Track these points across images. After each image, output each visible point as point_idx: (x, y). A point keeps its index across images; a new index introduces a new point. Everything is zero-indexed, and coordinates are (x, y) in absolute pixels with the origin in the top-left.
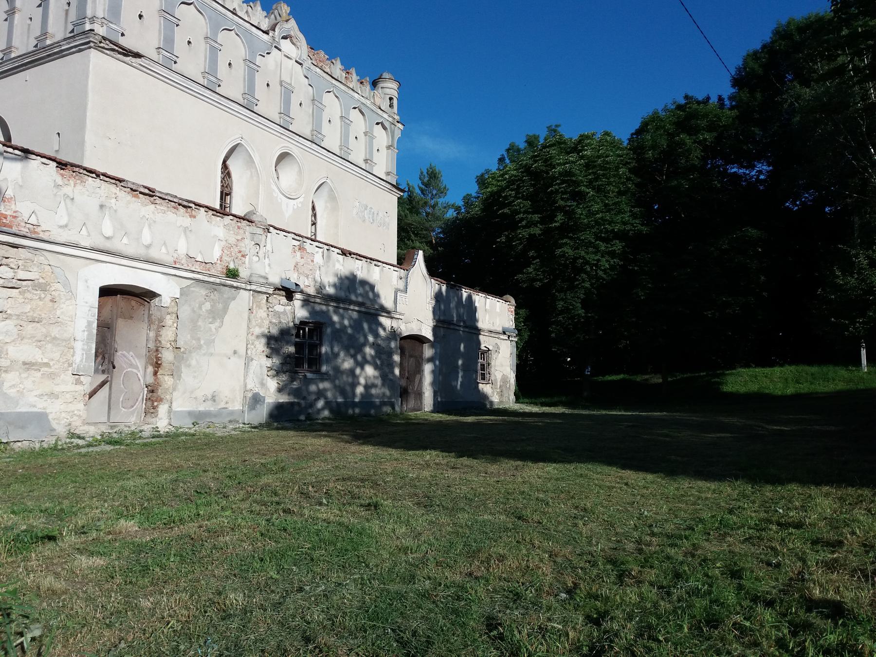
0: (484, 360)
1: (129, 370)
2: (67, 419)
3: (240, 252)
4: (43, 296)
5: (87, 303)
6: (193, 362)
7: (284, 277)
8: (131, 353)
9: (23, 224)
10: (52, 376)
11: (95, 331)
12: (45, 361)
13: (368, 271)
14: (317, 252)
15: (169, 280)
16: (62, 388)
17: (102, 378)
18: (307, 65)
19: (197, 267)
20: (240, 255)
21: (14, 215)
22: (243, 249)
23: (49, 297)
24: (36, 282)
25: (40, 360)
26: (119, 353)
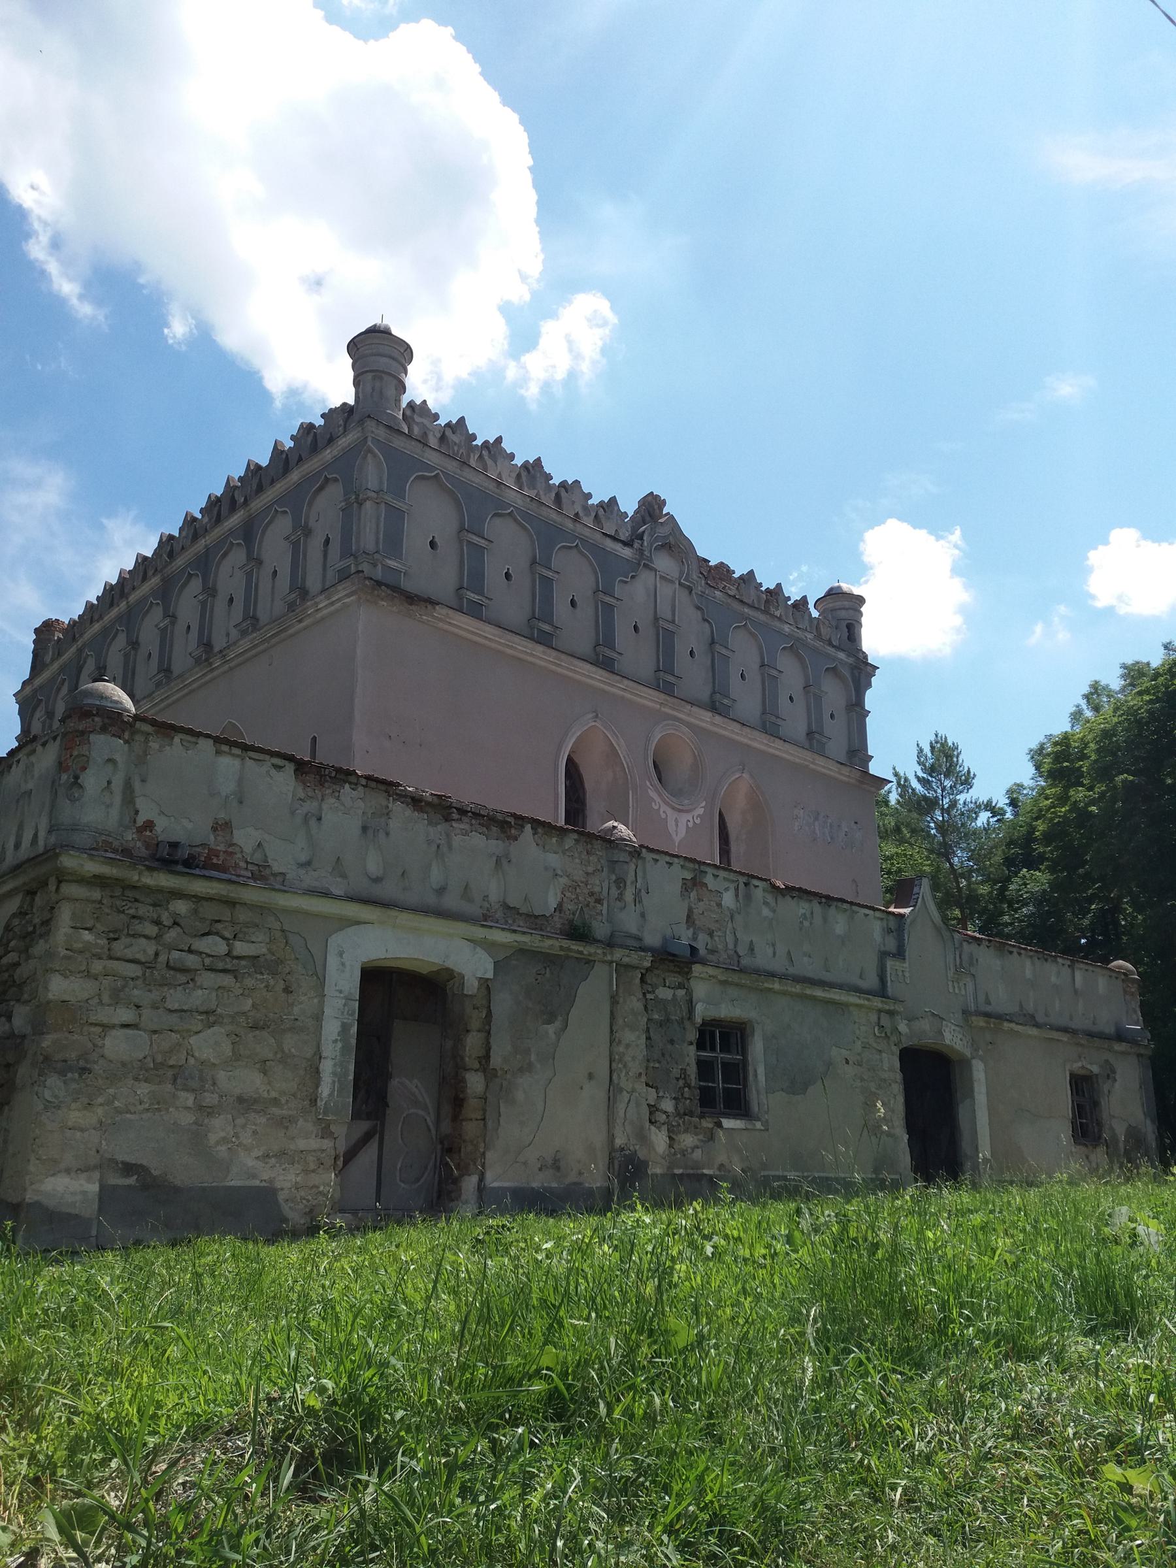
0: (1084, 1096)
1: (412, 1111)
2: (308, 1201)
3: (592, 894)
4: (272, 982)
5: (341, 992)
6: (520, 1096)
7: (669, 933)
8: (416, 1081)
9: (243, 864)
10: (284, 1123)
11: (354, 1042)
12: (274, 1094)
13: (825, 920)
14: (727, 889)
15: (475, 948)
16: (302, 1144)
17: (364, 1126)
19: (521, 924)
20: (591, 900)
21: (230, 850)
22: (597, 889)
23: (281, 985)
24: (262, 959)
25: (265, 1095)
26: (394, 1083)
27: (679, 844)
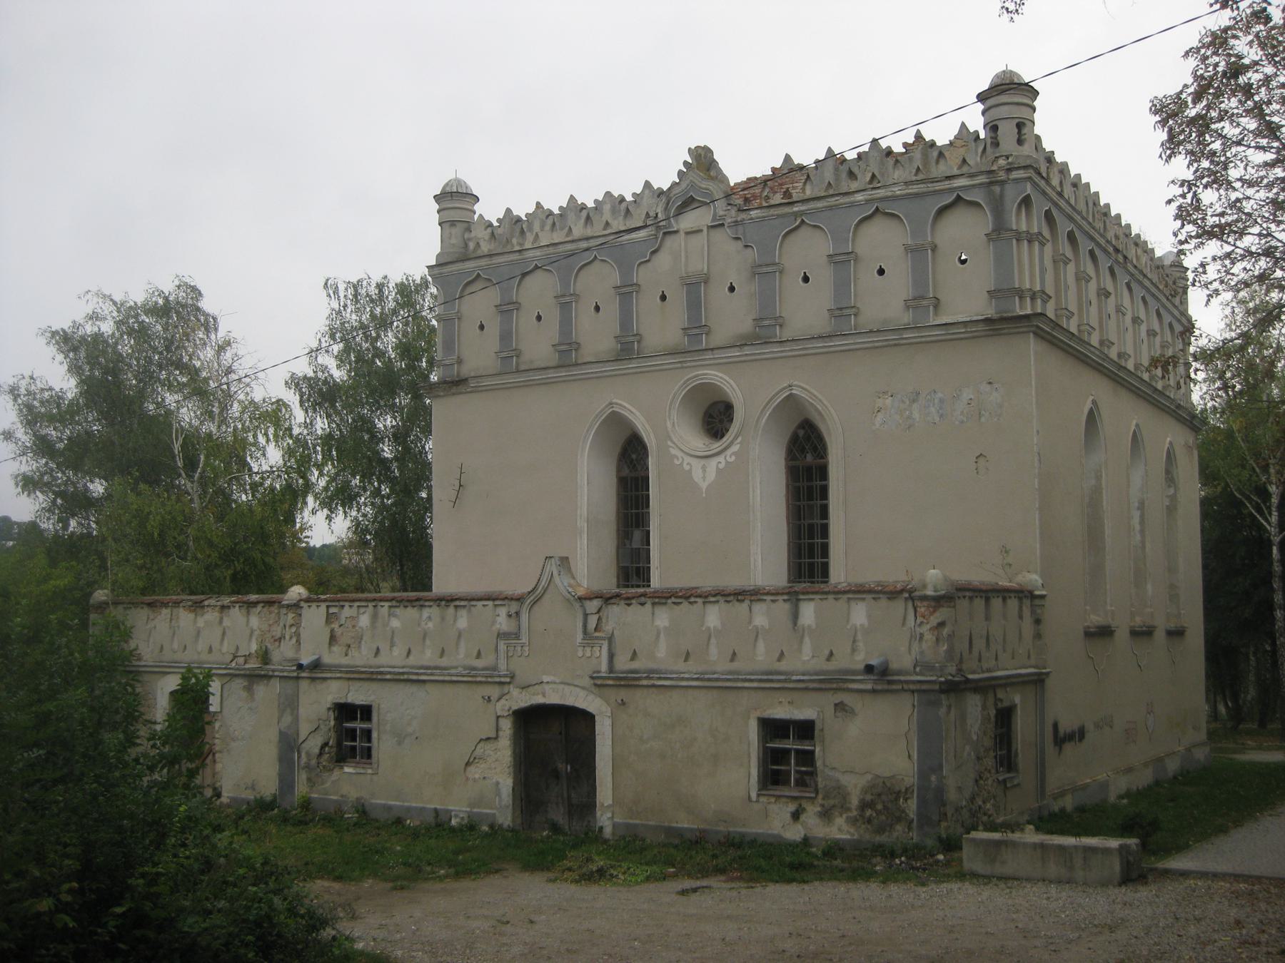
18: (730, 220)
27: (707, 488)
